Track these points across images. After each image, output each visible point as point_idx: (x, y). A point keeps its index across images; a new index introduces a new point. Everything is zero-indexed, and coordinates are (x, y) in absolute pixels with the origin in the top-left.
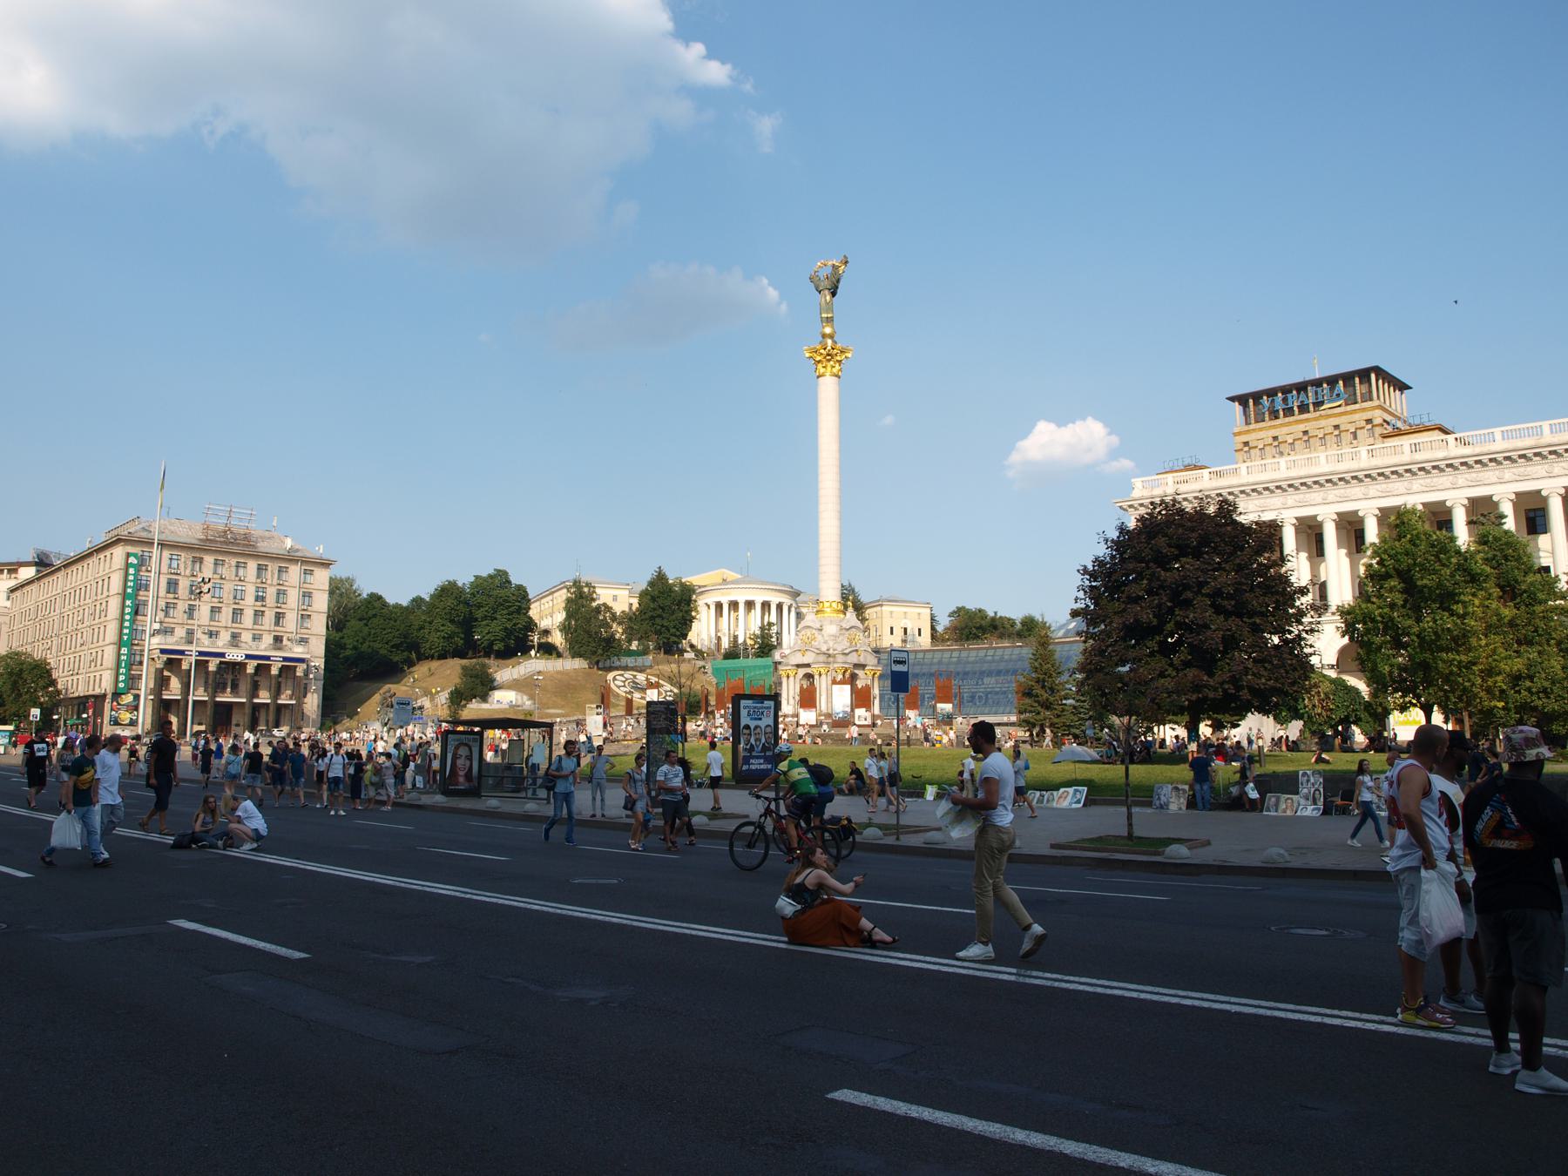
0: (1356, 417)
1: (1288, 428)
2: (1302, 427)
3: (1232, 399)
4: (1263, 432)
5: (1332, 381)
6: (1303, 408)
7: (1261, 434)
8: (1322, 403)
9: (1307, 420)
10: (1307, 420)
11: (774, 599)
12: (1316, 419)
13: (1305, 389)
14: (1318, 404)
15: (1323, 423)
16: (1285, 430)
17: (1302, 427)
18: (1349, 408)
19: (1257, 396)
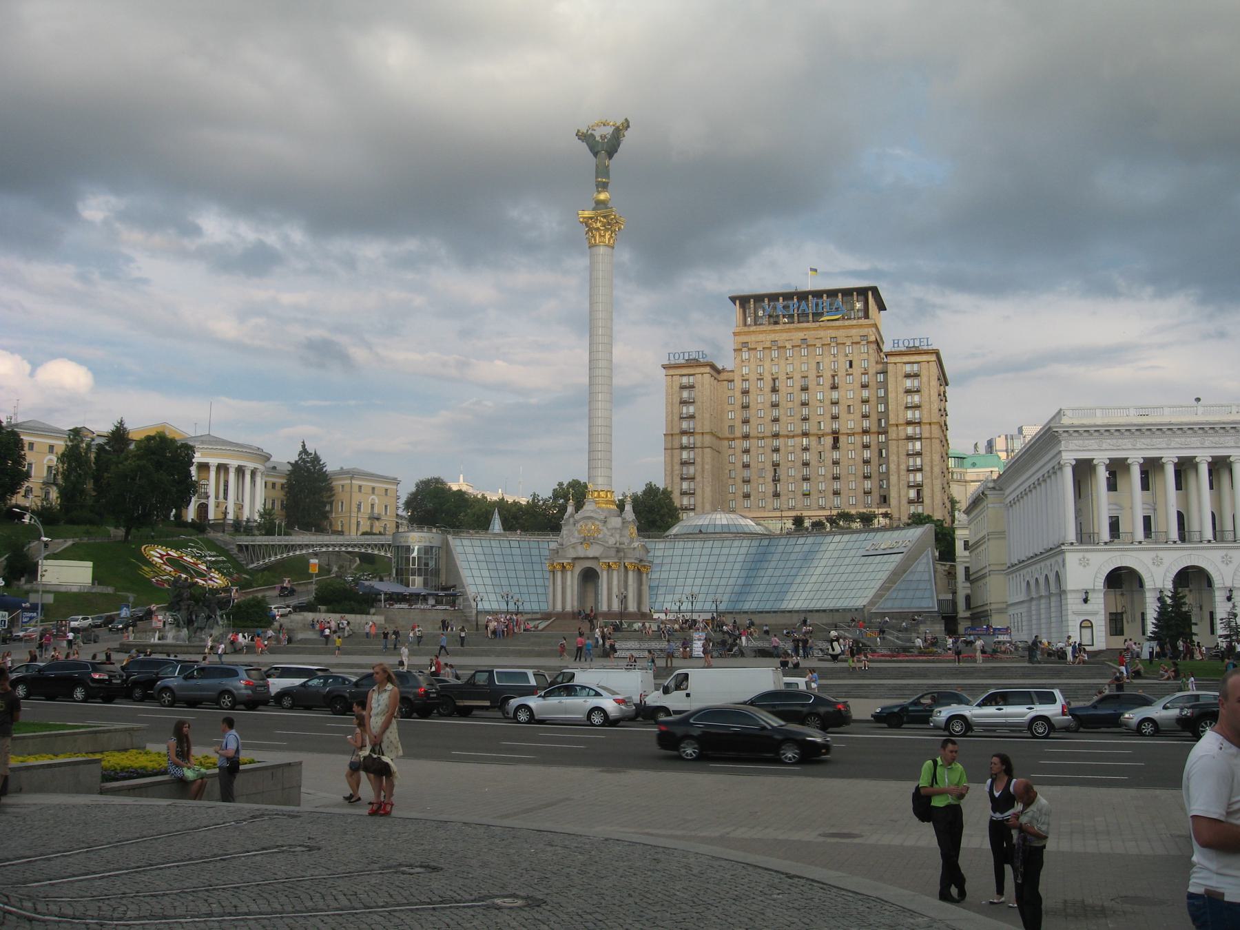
0: (853, 332)
1: (788, 334)
2: (801, 335)
3: (733, 299)
4: (764, 335)
5: (832, 294)
6: (803, 316)
7: (761, 337)
8: (822, 314)
9: (807, 329)
10: (807, 329)
11: (250, 465)
12: (815, 329)
13: (807, 298)
14: (817, 315)
15: (822, 333)
16: (785, 336)
17: (801, 335)
18: (847, 323)
19: (759, 298)
